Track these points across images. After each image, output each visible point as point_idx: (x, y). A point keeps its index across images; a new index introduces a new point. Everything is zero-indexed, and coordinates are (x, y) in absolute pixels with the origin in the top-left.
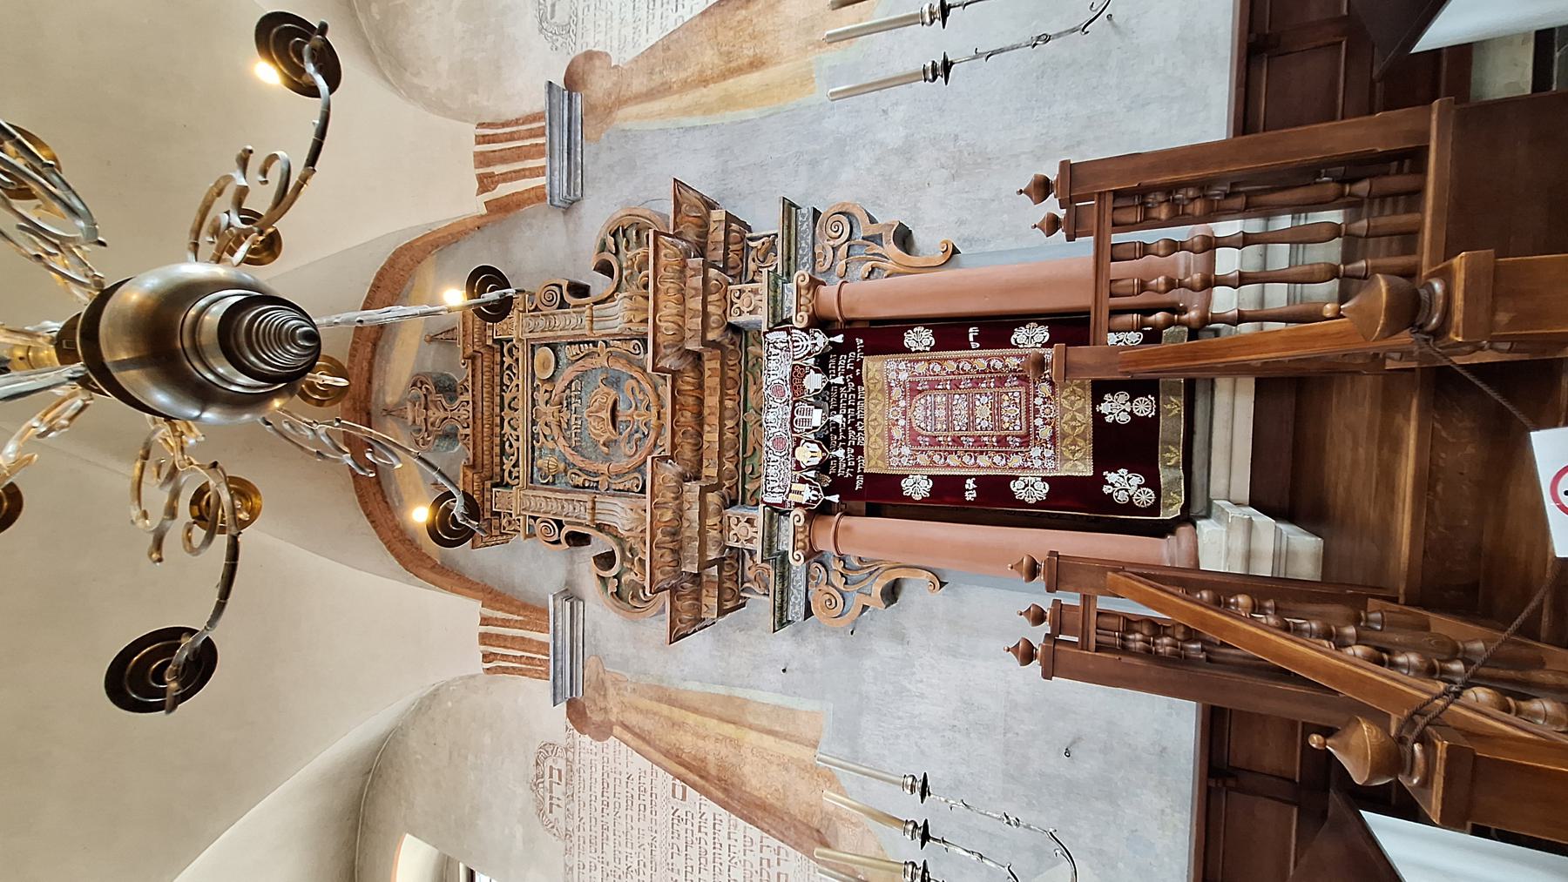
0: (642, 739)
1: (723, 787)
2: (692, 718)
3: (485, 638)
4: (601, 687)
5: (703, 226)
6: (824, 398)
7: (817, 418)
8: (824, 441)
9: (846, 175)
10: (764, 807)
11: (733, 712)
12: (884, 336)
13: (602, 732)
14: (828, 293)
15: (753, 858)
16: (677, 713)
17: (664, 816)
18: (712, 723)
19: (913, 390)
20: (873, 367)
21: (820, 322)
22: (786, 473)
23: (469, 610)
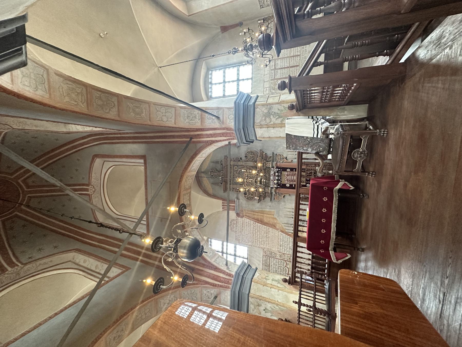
0: (249, 217)
1: (261, 222)
2: (256, 214)
3: (223, 205)
4: (242, 211)
5: (262, 155)
6: (278, 176)
7: (277, 178)
8: (277, 180)
9: (279, 149)
10: (267, 223)
11: (263, 212)
12: (285, 169)
13: (242, 217)
14: (278, 164)
15: (265, 230)
16: (254, 213)
17: (252, 226)
18: (260, 214)
19: (287, 175)
20: (283, 172)
21: (277, 168)
22: (273, 184)
23: (220, 202)
